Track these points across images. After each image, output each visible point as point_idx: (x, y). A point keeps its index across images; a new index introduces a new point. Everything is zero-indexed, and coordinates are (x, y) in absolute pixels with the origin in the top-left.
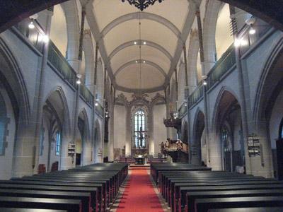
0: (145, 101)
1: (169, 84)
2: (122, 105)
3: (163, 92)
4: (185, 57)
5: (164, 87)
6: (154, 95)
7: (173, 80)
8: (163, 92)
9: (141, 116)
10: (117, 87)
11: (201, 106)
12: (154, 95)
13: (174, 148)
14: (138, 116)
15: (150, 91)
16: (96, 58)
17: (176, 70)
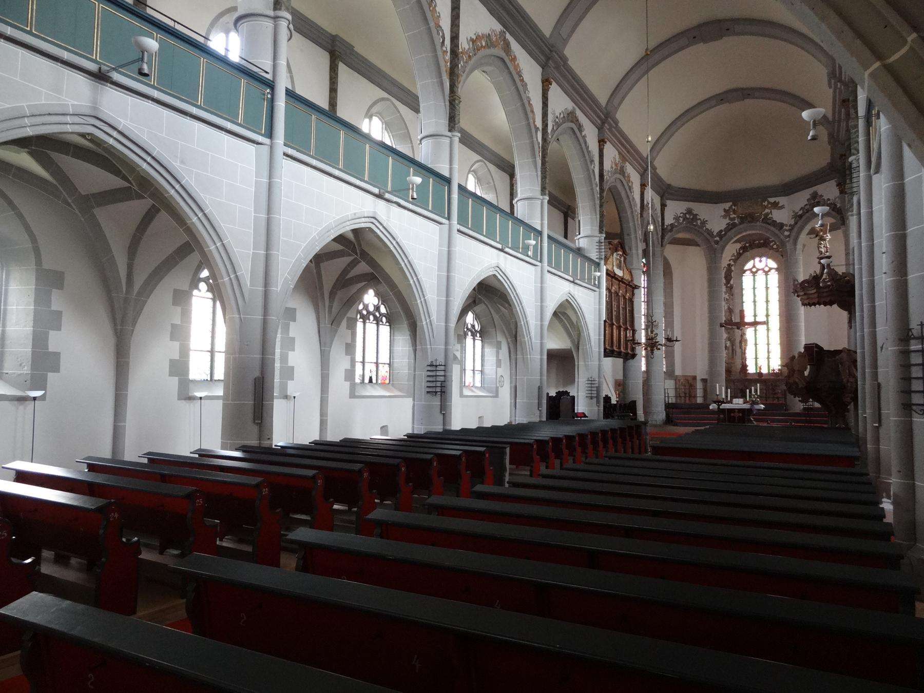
0: (774, 224)
3: (833, 183)
6: (801, 199)
8: (833, 183)
9: (766, 273)
10: (666, 192)
14: (754, 274)
15: (789, 189)
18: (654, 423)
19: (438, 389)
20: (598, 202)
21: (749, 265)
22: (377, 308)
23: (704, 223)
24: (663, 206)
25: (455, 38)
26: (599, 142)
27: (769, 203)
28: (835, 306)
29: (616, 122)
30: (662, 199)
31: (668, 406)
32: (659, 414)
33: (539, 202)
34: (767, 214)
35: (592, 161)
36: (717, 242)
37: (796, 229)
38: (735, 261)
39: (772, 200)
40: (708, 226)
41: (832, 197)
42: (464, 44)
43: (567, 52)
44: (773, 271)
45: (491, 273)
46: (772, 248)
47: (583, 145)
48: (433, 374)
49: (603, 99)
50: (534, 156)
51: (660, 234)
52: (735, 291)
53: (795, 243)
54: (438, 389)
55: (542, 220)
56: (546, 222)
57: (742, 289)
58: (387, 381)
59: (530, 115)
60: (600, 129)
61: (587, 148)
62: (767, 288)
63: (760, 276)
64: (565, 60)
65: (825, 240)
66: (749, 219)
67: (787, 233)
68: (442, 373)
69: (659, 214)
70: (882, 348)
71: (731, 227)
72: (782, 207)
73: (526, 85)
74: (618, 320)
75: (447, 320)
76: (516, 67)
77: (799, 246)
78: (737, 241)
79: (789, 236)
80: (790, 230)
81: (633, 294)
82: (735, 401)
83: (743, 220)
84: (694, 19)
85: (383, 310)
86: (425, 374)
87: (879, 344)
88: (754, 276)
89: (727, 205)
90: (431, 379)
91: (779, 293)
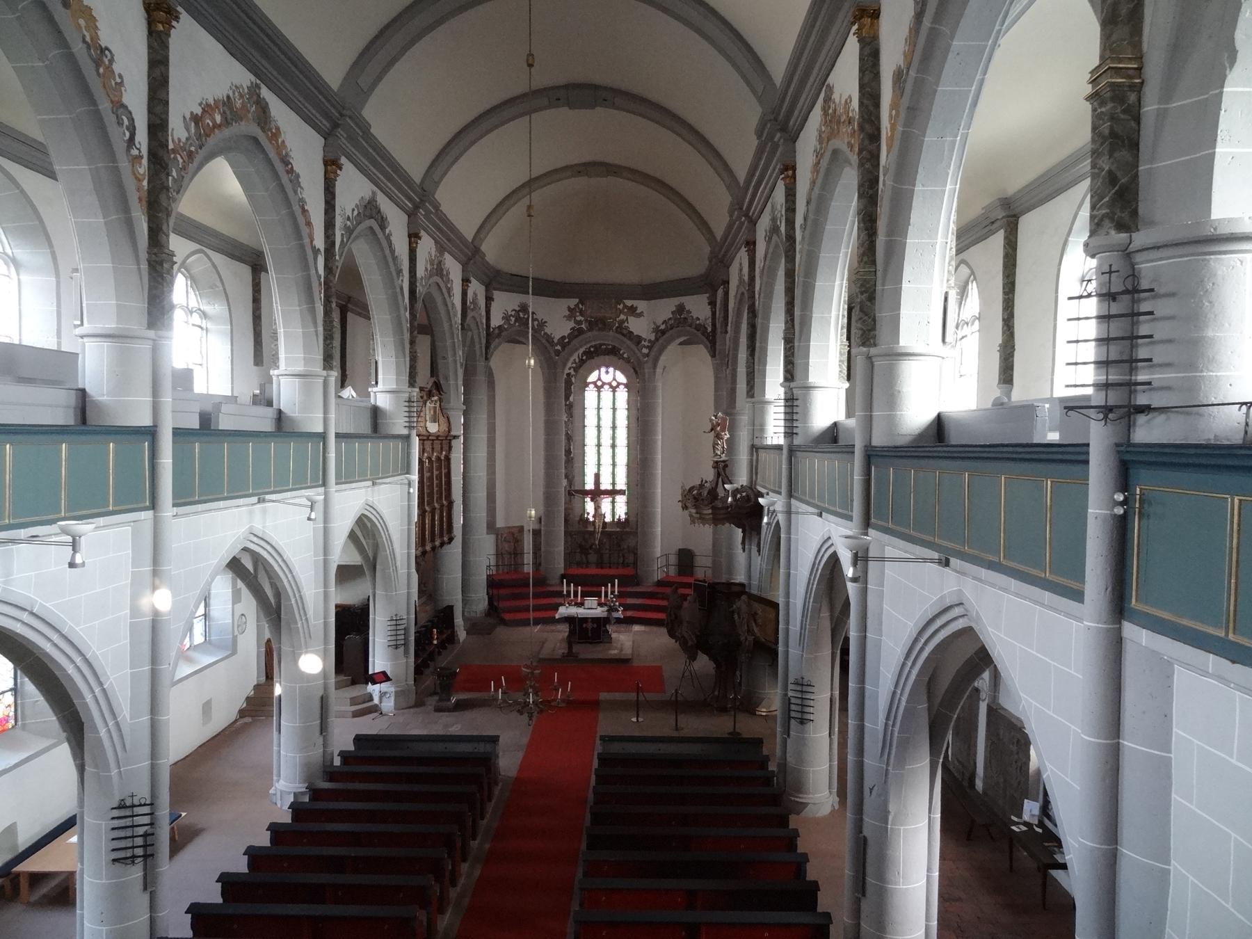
6: (663, 309)
9: (614, 389)
10: (495, 280)
12: (663, 309)
14: (599, 389)
15: (652, 291)
18: (473, 614)
19: (139, 852)
21: (593, 377)
24: (489, 299)
25: (158, 127)
26: (410, 236)
27: (625, 306)
29: (437, 207)
30: (487, 291)
31: (492, 583)
32: (481, 600)
33: (321, 381)
34: (622, 322)
35: (399, 272)
36: (558, 353)
37: (655, 349)
38: (576, 370)
39: (629, 303)
40: (548, 330)
42: (178, 130)
43: (368, 113)
44: (622, 387)
46: (621, 357)
47: (387, 252)
48: (128, 822)
49: (416, 174)
51: (484, 341)
53: (655, 366)
54: (139, 852)
57: (584, 409)
59: (305, 231)
60: (411, 215)
61: (392, 252)
62: (614, 409)
63: (607, 394)
64: (365, 128)
67: (645, 351)
68: (146, 820)
69: (484, 313)
70: (871, 790)
71: (576, 333)
72: (641, 315)
73: (298, 176)
74: (431, 495)
76: (280, 148)
77: (659, 370)
79: (647, 355)
83: (592, 325)
86: (105, 824)
87: (867, 784)
88: (599, 392)
89: (573, 302)
90: (122, 834)
91: (628, 417)
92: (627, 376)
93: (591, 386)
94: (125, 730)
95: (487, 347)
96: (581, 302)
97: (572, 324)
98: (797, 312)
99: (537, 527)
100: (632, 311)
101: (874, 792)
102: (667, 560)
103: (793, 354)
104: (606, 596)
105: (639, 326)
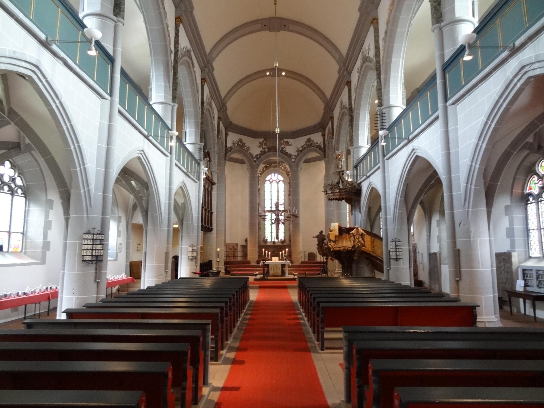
0: (286, 154)
1: (332, 118)
2: (242, 162)
4: (377, 41)
5: (321, 127)
6: (301, 142)
7: (342, 107)
8: (320, 134)
9: (278, 183)
10: (230, 127)
11: (428, 144)
13: (347, 244)
14: (271, 183)
15: (296, 134)
16: (177, 43)
17: (349, 83)
20: (200, 120)
21: (268, 178)
22: (13, 180)
23: (248, 148)
27: (284, 141)
28: (344, 201)
33: (170, 107)
34: (283, 148)
36: (255, 162)
38: (261, 174)
40: (251, 151)
41: (319, 142)
44: (281, 182)
45: (138, 155)
47: (194, 78)
50: (167, 72)
52: (261, 192)
55: (172, 121)
56: (175, 123)
58: (20, 250)
65: (341, 161)
66: (274, 150)
67: (293, 160)
71: (263, 153)
72: (291, 145)
75: (105, 190)
78: (264, 163)
79: (294, 162)
80: (295, 159)
81: (212, 188)
82: (274, 258)
83: (270, 150)
84: (267, 12)
85: (19, 182)
89: (261, 140)
92: (283, 177)
93: (268, 182)
94: (92, 196)
95: (226, 154)
96: (265, 140)
97: (261, 149)
98: (382, 77)
99: (244, 244)
100: (287, 143)
101: (462, 225)
102: (305, 254)
103: (381, 96)
104: (282, 256)
105: (291, 150)
